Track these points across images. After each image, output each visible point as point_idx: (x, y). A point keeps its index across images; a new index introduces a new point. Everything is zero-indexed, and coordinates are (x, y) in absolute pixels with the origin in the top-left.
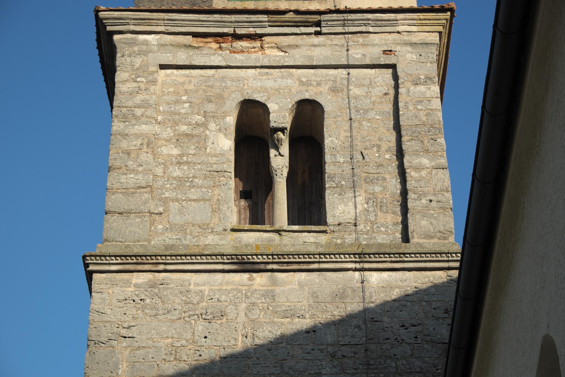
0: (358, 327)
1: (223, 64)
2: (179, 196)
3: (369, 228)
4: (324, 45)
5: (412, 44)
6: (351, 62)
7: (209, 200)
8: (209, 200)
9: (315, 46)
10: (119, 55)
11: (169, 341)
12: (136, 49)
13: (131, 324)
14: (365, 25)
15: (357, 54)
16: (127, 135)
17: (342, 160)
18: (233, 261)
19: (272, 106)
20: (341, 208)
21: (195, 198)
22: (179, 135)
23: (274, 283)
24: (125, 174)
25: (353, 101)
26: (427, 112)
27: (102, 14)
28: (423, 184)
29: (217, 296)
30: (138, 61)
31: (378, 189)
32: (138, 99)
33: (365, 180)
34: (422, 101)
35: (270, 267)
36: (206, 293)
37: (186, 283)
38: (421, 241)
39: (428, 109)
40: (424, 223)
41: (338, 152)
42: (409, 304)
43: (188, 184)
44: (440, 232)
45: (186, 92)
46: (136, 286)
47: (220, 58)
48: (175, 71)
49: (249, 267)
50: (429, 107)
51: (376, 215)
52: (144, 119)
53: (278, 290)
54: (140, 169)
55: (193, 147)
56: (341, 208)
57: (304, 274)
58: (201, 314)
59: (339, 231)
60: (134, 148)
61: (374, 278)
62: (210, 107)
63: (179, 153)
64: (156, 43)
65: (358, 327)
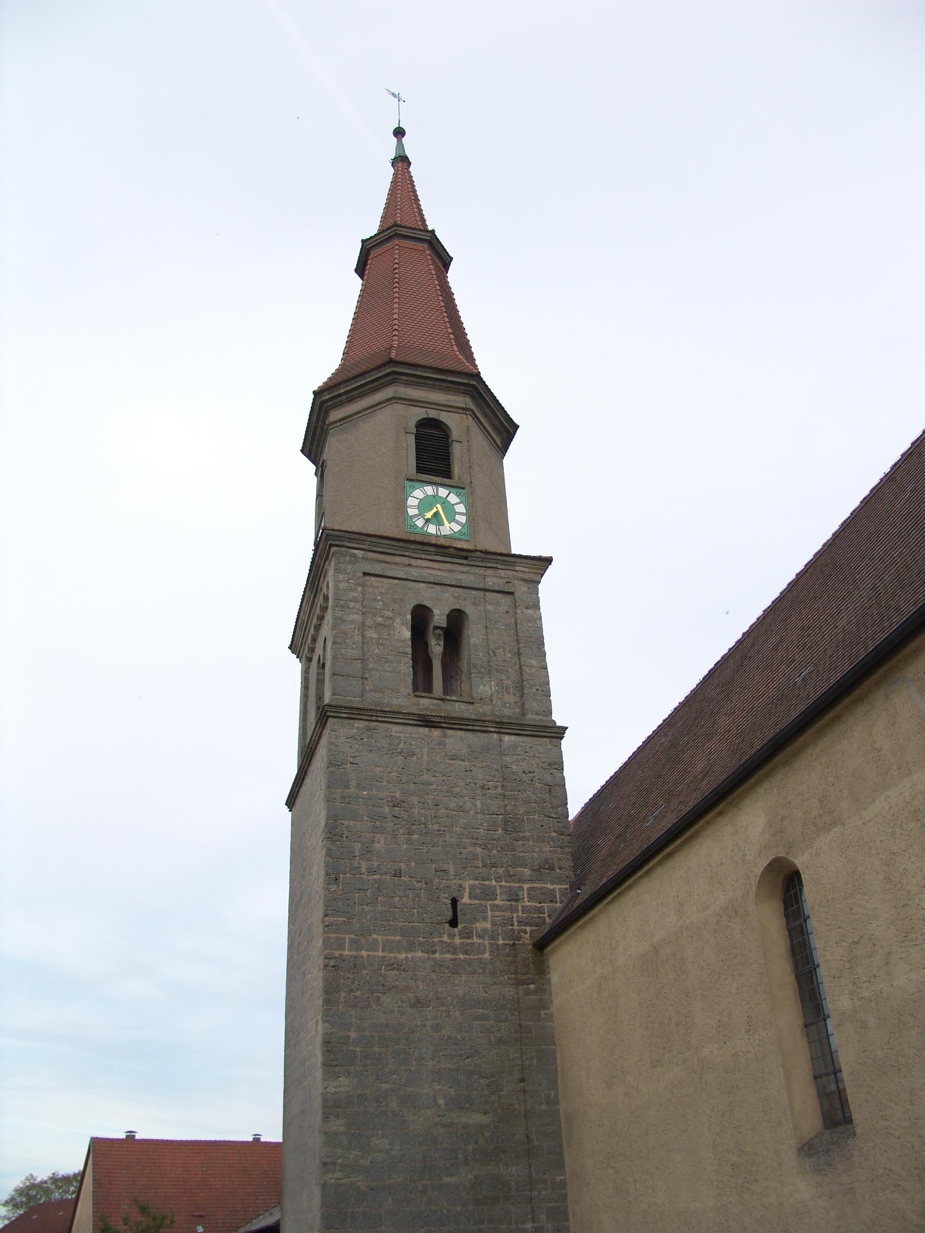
0: (497, 770)
1: (404, 577)
2: (379, 668)
3: (499, 703)
4: (470, 573)
5: (525, 580)
6: (487, 588)
7: (398, 673)
8: (398, 673)
9: (463, 573)
11: (380, 769)
13: (356, 755)
14: (496, 563)
15: (490, 582)
16: (344, 620)
17: (481, 655)
18: (420, 719)
19: (436, 612)
20: (482, 687)
21: (389, 670)
22: (376, 624)
23: (445, 736)
24: (345, 648)
25: (487, 614)
26: (534, 628)
28: (533, 678)
29: (409, 741)
31: (503, 677)
33: (496, 670)
34: (531, 621)
35: (443, 725)
36: (403, 739)
37: (390, 730)
38: (534, 717)
39: (535, 627)
40: (535, 704)
41: (479, 649)
42: (527, 758)
43: (383, 660)
44: (544, 711)
45: (380, 593)
46: (357, 728)
47: (402, 573)
49: (429, 724)
50: (536, 625)
51: (503, 695)
52: (354, 611)
53: (447, 741)
54: (354, 646)
55: (386, 634)
56: (482, 687)
57: (463, 733)
58: (400, 753)
59: (480, 703)
60: (348, 630)
61: (507, 738)
62: (396, 606)
63: (377, 636)
64: (361, 557)
65: (497, 770)
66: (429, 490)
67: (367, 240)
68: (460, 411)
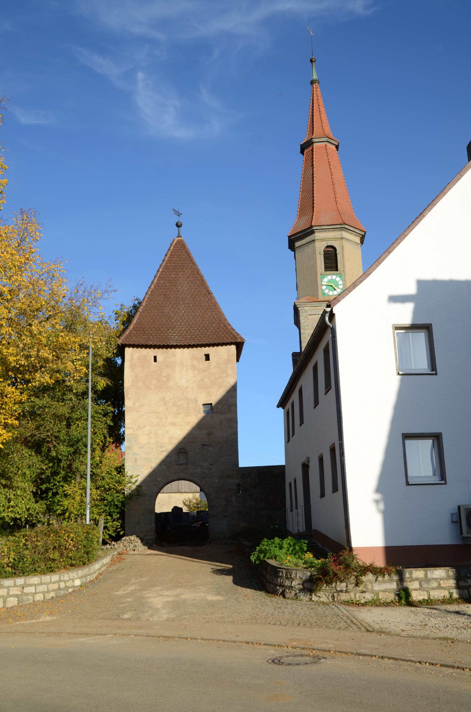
12: (303, 311)
27: (296, 304)
30: (304, 314)
32: (306, 324)
66: (329, 277)
67: (302, 145)
68: (340, 239)
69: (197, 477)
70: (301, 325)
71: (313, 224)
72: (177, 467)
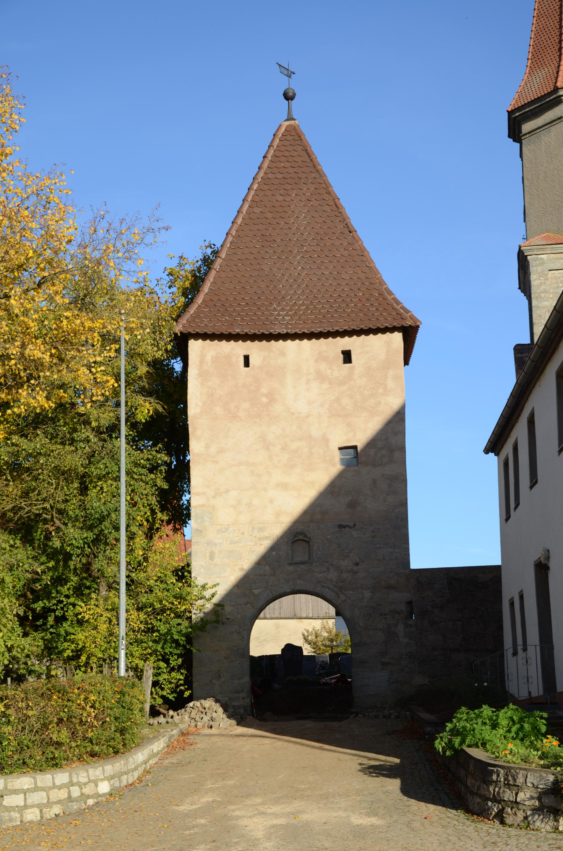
10: (531, 266)
12: (538, 262)
27: (522, 248)
30: (539, 269)
32: (542, 288)
48: (555, 271)
69: (328, 588)
70: (532, 291)
71: (559, 84)
72: (291, 568)
